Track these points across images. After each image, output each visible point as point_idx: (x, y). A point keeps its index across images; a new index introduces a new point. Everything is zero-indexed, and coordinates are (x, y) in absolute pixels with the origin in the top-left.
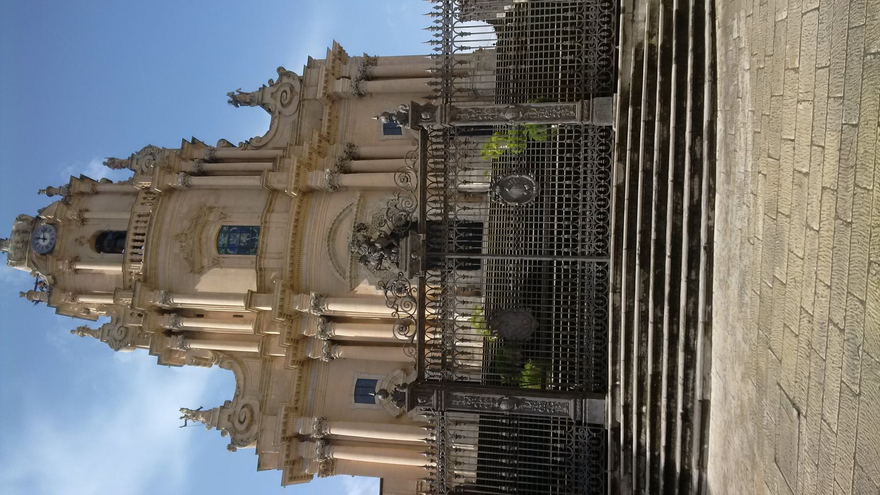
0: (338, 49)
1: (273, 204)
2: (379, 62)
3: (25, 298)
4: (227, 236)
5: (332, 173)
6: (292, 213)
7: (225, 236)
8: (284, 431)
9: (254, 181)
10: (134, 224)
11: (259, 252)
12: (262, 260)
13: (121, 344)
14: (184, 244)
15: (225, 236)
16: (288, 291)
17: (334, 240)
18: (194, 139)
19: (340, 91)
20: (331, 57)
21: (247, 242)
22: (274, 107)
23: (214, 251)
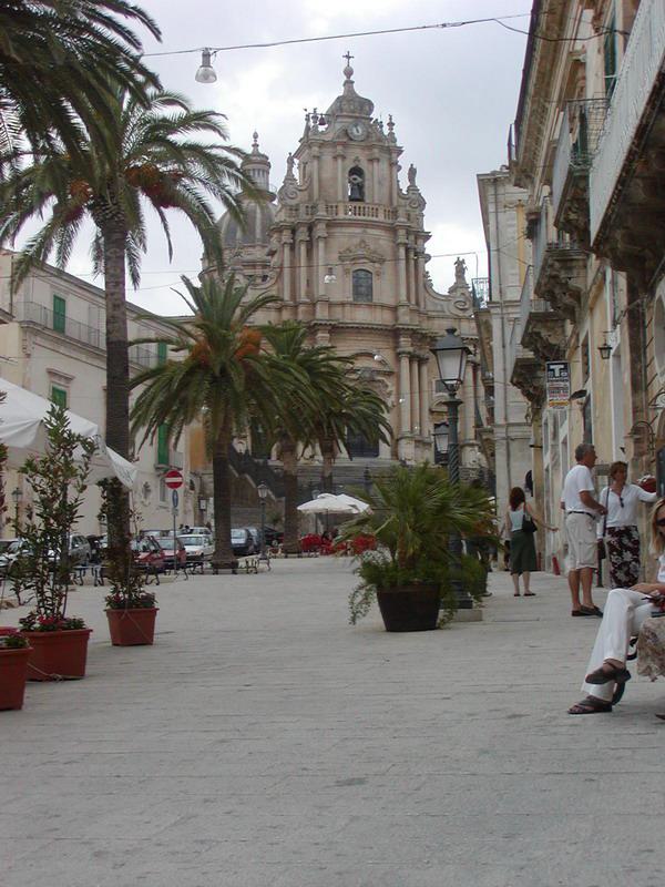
5: (409, 353)
9: (403, 297)
16: (329, 328)
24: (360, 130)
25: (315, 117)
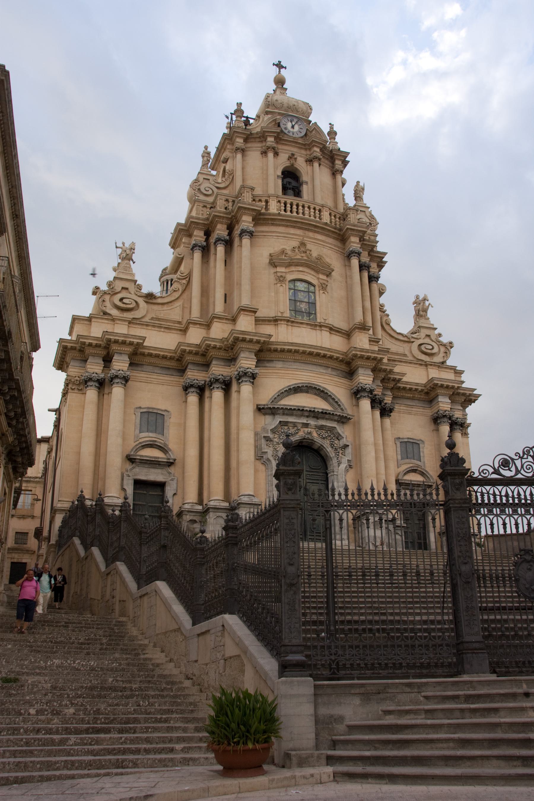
0: (473, 398)
1: (337, 334)
2: (465, 439)
3: (236, 108)
5: (371, 391)
7: (305, 288)
8: (116, 342)
10: (312, 206)
12: (286, 323)
13: (197, 190)
15: (305, 288)
16: (257, 347)
18: (386, 262)
19: (440, 400)
20: (468, 393)
22: (419, 337)
23: (290, 277)
24: (297, 128)
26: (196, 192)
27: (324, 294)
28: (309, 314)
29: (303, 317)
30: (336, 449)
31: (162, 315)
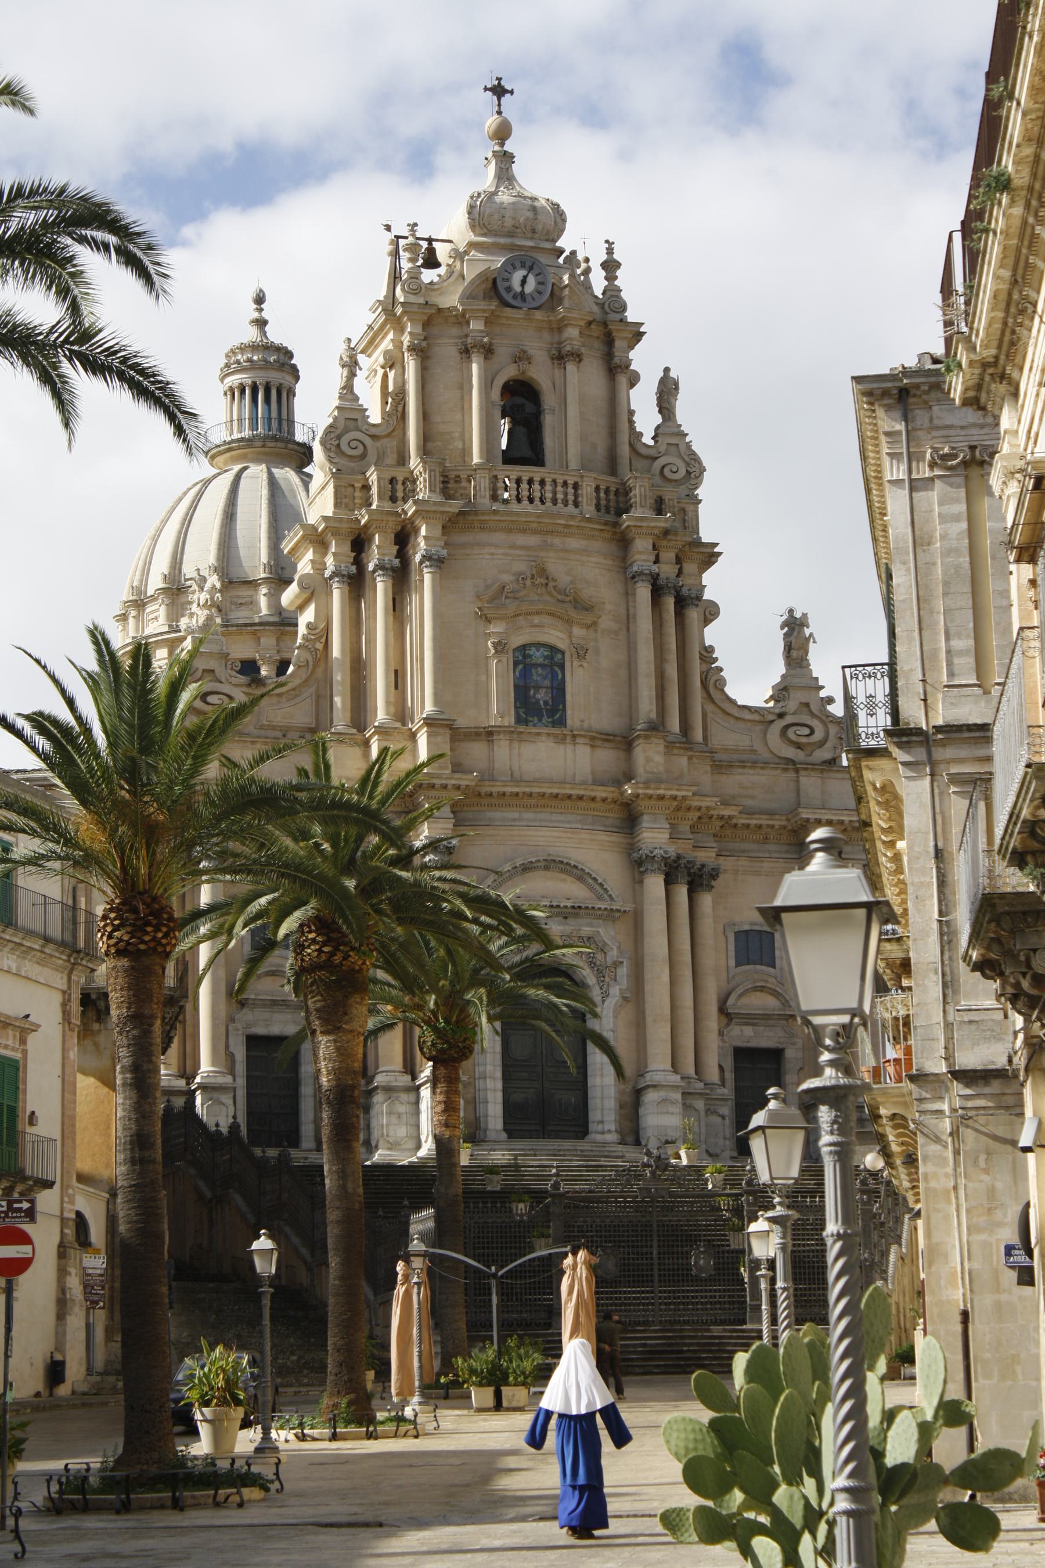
4: (546, 662)
6: (592, 790)
7: (546, 657)
11: (521, 728)
13: (333, 449)
14: (528, 582)
17: (547, 868)
18: (720, 554)
21: (538, 701)
23: (517, 641)
25: (413, 248)
26: (332, 455)
27: (581, 669)
28: (552, 712)
29: (540, 720)
30: (599, 971)
31: (279, 719)
